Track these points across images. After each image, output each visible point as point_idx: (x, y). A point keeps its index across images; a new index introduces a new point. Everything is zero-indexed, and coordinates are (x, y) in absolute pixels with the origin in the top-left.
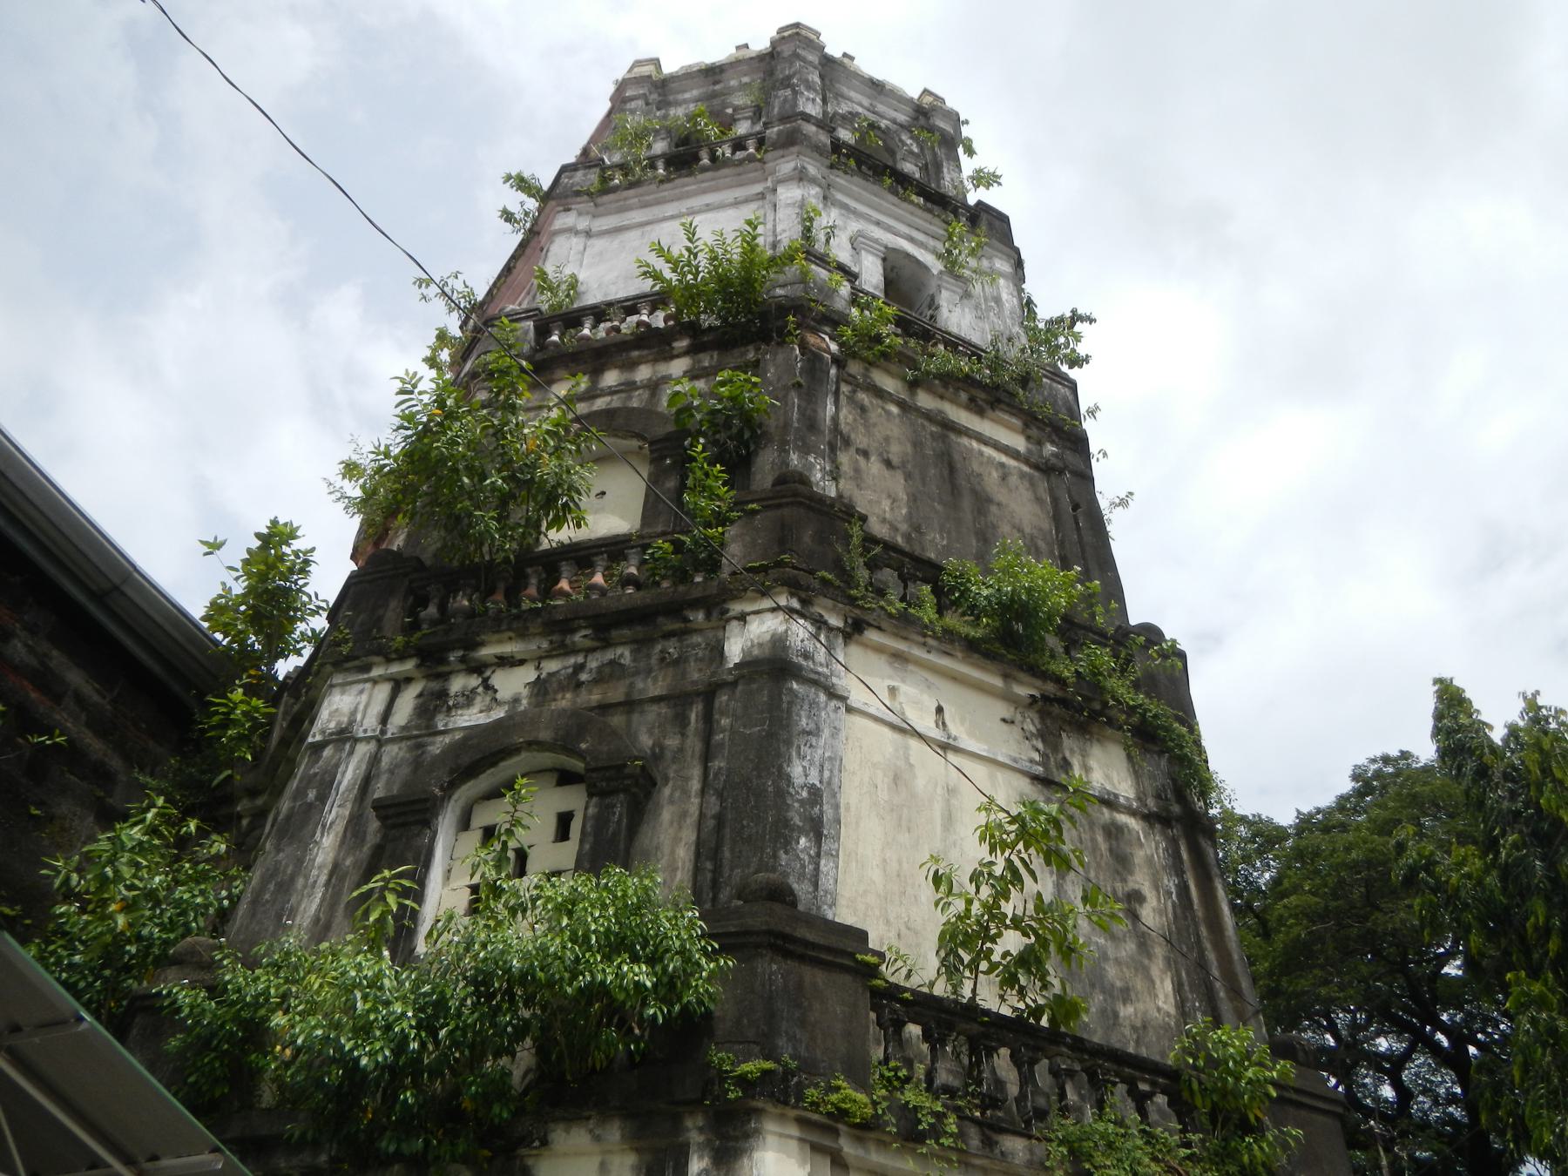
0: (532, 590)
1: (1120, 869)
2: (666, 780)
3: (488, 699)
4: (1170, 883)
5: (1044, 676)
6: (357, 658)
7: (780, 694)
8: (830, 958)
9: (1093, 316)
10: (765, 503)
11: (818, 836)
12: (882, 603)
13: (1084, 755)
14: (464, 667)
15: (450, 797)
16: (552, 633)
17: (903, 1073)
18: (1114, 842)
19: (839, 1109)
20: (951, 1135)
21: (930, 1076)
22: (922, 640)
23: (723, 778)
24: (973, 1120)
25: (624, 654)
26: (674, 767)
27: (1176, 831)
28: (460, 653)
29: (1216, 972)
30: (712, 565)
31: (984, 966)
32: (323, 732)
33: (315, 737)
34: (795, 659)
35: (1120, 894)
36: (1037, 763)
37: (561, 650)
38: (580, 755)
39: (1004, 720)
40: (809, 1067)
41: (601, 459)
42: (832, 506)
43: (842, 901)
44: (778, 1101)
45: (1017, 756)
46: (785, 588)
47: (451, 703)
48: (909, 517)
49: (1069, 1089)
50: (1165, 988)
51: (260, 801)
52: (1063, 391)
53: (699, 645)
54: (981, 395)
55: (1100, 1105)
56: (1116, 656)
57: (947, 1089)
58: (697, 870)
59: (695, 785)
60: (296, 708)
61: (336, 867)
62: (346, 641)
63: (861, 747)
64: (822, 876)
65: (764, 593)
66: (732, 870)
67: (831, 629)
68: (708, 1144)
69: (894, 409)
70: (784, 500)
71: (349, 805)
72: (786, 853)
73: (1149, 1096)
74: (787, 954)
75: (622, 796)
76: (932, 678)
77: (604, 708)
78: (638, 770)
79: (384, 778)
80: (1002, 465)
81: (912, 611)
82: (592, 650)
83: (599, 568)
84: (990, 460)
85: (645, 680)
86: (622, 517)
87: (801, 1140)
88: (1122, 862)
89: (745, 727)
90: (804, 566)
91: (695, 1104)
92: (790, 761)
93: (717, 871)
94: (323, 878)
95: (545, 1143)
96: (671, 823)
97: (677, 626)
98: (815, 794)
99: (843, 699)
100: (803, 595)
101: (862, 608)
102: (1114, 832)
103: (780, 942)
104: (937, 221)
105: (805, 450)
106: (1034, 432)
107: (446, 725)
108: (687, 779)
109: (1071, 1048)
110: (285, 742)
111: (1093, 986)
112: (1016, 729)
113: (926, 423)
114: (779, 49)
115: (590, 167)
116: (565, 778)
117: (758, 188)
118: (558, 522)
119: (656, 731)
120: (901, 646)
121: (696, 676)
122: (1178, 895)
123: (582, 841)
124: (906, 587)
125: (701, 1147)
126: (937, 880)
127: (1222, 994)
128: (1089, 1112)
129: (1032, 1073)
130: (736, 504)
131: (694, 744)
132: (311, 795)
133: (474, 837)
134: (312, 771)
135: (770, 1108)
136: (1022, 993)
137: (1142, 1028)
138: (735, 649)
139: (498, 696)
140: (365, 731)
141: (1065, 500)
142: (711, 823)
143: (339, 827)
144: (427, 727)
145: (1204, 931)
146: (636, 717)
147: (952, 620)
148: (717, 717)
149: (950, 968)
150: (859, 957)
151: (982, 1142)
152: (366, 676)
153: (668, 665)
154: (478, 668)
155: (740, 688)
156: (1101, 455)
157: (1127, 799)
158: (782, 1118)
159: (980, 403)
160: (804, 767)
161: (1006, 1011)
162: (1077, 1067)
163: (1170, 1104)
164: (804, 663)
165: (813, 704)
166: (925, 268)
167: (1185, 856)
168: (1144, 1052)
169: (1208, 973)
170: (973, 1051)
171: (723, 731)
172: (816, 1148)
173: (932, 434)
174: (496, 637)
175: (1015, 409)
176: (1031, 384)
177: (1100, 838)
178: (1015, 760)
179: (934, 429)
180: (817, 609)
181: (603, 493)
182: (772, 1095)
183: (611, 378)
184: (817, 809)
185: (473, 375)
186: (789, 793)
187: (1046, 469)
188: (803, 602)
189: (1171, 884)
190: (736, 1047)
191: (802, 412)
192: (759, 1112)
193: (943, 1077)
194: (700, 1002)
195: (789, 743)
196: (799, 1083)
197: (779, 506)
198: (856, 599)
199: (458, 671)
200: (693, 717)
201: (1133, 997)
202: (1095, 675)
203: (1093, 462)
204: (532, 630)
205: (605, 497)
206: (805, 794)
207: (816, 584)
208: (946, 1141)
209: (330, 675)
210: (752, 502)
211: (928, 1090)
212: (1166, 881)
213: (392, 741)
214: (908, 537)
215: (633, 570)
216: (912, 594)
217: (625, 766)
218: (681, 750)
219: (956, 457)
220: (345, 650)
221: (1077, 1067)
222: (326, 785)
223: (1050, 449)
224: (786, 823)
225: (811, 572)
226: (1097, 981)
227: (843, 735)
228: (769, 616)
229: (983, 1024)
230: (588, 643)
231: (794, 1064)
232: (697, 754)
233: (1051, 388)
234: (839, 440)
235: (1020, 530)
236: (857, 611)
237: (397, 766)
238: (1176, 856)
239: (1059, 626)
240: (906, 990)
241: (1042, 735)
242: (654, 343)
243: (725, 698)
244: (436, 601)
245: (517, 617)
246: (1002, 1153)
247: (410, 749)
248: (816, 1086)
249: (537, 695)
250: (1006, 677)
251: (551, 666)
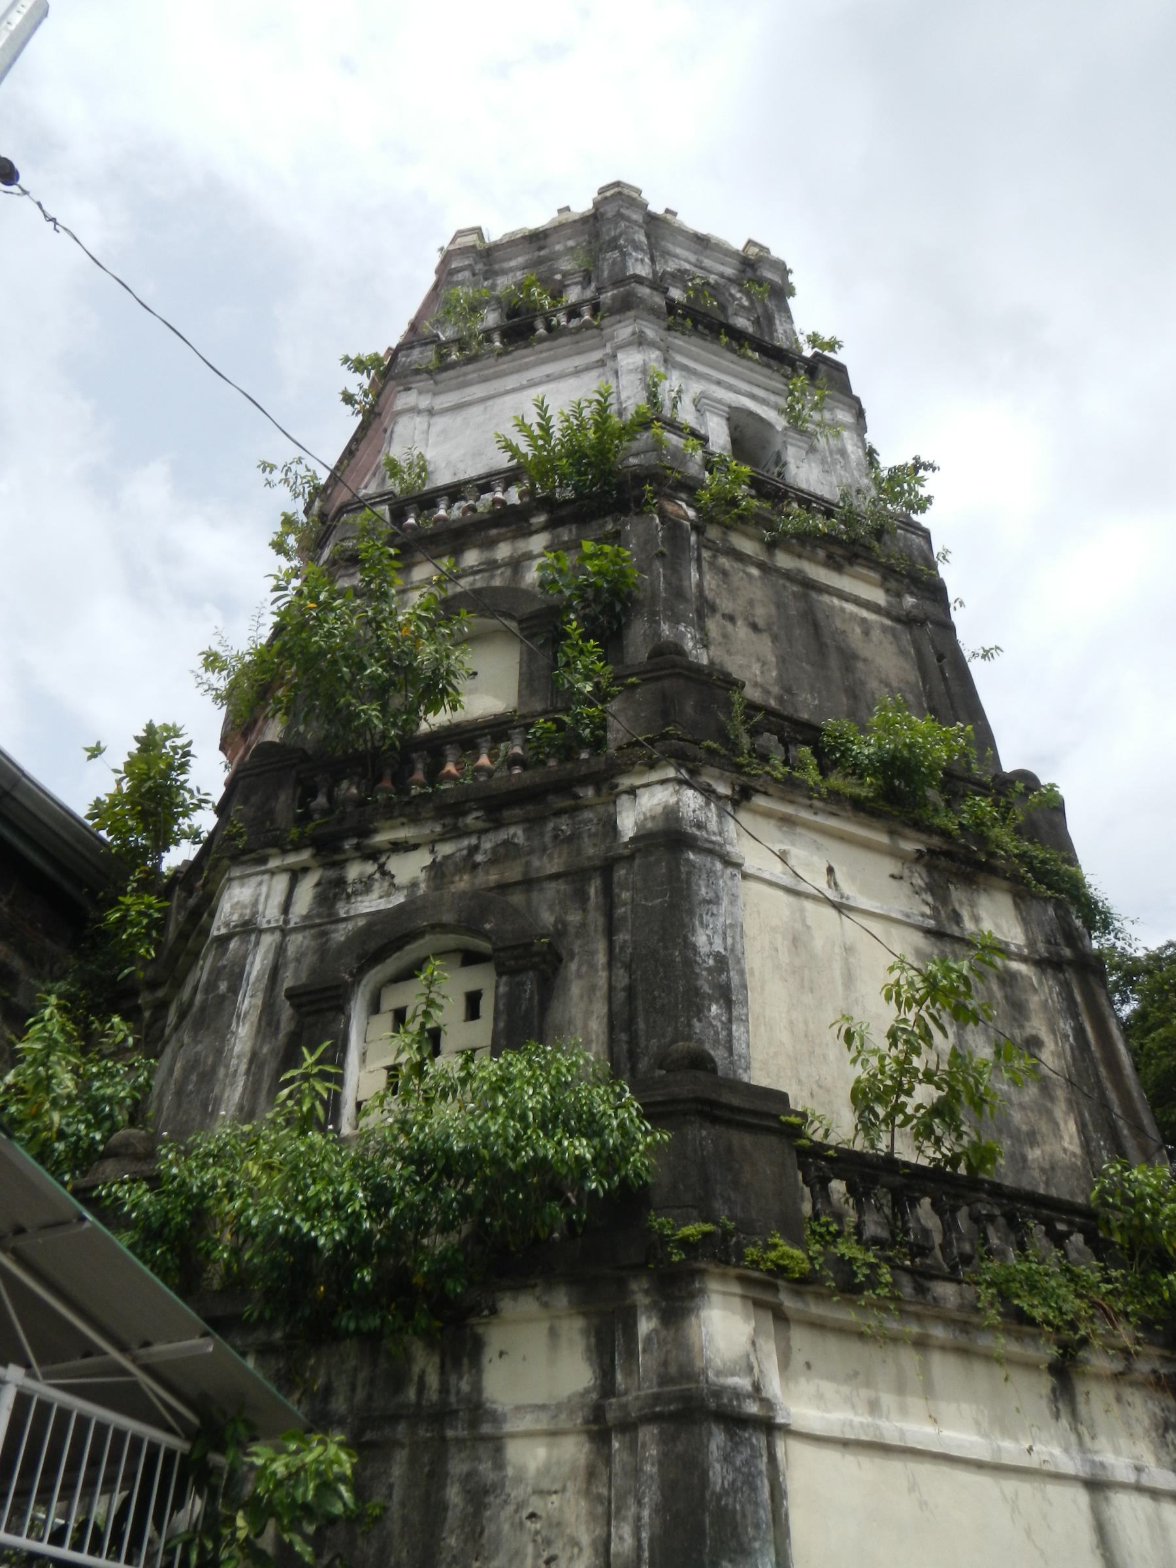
0: (419, 775)
1: (1017, 1016)
2: (572, 956)
3: (386, 884)
4: (1066, 1026)
5: (930, 830)
6: (252, 851)
7: (678, 865)
8: (755, 1121)
9: (936, 465)
10: (645, 676)
11: (728, 1004)
12: (768, 769)
13: (973, 905)
14: (358, 854)
15: (359, 982)
16: (443, 817)
17: (834, 1228)
18: (1009, 990)
19: (778, 1266)
20: (886, 1285)
21: (859, 1229)
22: (808, 802)
23: (629, 951)
24: (905, 1269)
25: (517, 833)
26: (579, 942)
27: (1070, 975)
28: (355, 841)
29: (1117, 1110)
30: (598, 744)
31: (899, 1119)
32: (227, 925)
33: (218, 929)
34: (689, 830)
35: (1019, 1040)
36: (929, 917)
38: (485, 935)
39: (893, 876)
40: (746, 1227)
41: (472, 639)
42: (710, 675)
43: (755, 1065)
44: (721, 1261)
45: (909, 911)
46: (672, 760)
47: (350, 890)
48: (780, 680)
49: (991, 1231)
50: (1070, 1127)
51: (160, 993)
52: (917, 541)
53: (591, 820)
54: (839, 551)
55: (1021, 1246)
56: (996, 804)
57: (876, 1241)
58: (612, 1043)
59: (601, 959)
60: (192, 902)
61: (254, 1056)
62: (241, 835)
63: (759, 913)
64: (735, 1041)
65: (652, 766)
66: (648, 1041)
67: (720, 797)
68: (654, 1305)
69: (755, 572)
70: (662, 673)
71: (260, 995)
72: (700, 1020)
73: (1067, 1235)
74: (715, 1120)
75: (531, 974)
76: (820, 839)
77: (503, 887)
78: (545, 948)
79: (292, 966)
80: (864, 621)
81: (796, 774)
82: (485, 831)
83: (484, 750)
84: (853, 617)
85: (541, 858)
86: (496, 697)
87: (743, 1297)
88: (1018, 1009)
89: (646, 900)
90: (689, 737)
91: (638, 1269)
92: (694, 930)
93: (633, 1041)
94: (243, 1067)
95: (494, 1311)
96: (582, 997)
97: (568, 803)
98: (721, 962)
99: (738, 866)
100: (691, 766)
101: (749, 775)
102: (1008, 979)
103: (707, 1109)
104: (776, 375)
105: (675, 620)
106: (893, 584)
107: (347, 912)
108: (592, 953)
109: (990, 1194)
110: (183, 936)
111: (1000, 1131)
112: (905, 885)
113: (788, 584)
114: (602, 210)
115: (426, 344)
116: (470, 958)
117: (597, 355)
118: (434, 707)
119: (557, 908)
120: (789, 810)
121: (591, 851)
122: (1075, 1039)
123: (496, 1020)
124: (787, 751)
125: (649, 1309)
126: (849, 1037)
127: (1125, 1132)
128: (1012, 1253)
129: (955, 1220)
130: (615, 678)
131: (596, 919)
132: (223, 987)
133: (385, 1020)
134: (220, 964)
135: (712, 1268)
136: (938, 1142)
137: (1050, 1170)
138: (628, 823)
139: (396, 881)
140: (269, 922)
141: (929, 651)
142: (621, 996)
143: (254, 1017)
144: (330, 915)
145: (1103, 1071)
146: (535, 895)
147: (836, 780)
148: (617, 891)
149: (866, 1125)
150: (783, 1118)
151: (915, 1289)
152: (263, 868)
153: (562, 841)
154: (373, 855)
155: (637, 862)
156: (957, 604)
157: (1018, 946)
158: (724, 1277)
159: (838, 559)
160: (708, 936)
161: (924, 1162)
162: (997, 1212)
163: (1086, 1242)
164: (698, 833)
165: (711, 873)
166: (768, 425)
167: (1079, 998)
168: (1054, 1193)
169: (1111, 1110)
170: (897, 1203)
171: (625, 904)
172: (758, 1304)
173: (794, 593)
174: (389, 823)
175: (874, 564)
176: (886, 537)
177: (995, 987)
178: (908, 916)
179: (795, 589)
180: (705, 779)
181: (475, 674)
182: (714, 1256)
183: (471, 558)
184: (724, 976)
185: (332, 562)
186: (696, 962)
187: (908, 621)
188: (693, 772)
189: (1068, 1027)
190: (676, 1212)
191: (668, 583)
192: (702, 1273)
193: (872, 1228)
194: (638, 1175)
195: (691, 913)
196: (738, 1243)
197: (659, 678)
198: (742, 766)
199: (353, 859)
200: (592, 891)
201: (1039, 1138)
202: (978, 825)
203: (952, 609)
204: (424, 815)
205: (477, 677)
206: (711, 962)
207: (702, 754)
208: (883, 1292)
209: (228, 869)
210: (631, 675)
211: (858, 1242)
212: (1062, 1024)
213: (296, 930)
214: (780, 699)
215: (518, 750)
216: (795, 758)
217: (532, 944)
218: (583, 925)
219: (820, 616)
220: (240, 843)
221: (997, 1212)
222: (236, 976)
223: (909, 601)
224: (697, 991)
225: (696, 743)
226: (1005, 1127)
227: (740, 902)
228: (659, 788)
229: (904, 1175)
230: (481, 825)
231: (731, 1225)
232: (600, 928)
233: (906, 539)
234: (705, 608)
235: (888, 685)
236: (744, 779)
237: (303, 954)
238: (1070, 1000)
239: (942, 781)
240: (830, 1147)
241: (930, 888)
243: (623, 872)
244: (324, 790)
245: (409, 803)
246: (934, 1299)
247: (315, 937)
248: (755, 1245)
249: (435, 877)
250: (892, 833)
251: (446, 849)
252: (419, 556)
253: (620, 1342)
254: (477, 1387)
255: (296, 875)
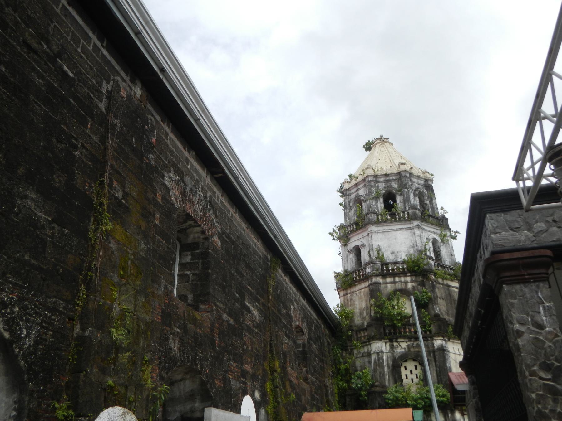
37: (410, 341)
59: (434, 365)
65: (439, 336)
69: (441, 286)
94: (387, 374)
117: (408, 226)
188: (444, 338)
207: (445, 335)
242: (403, 273)
251: (409, 343)
252: (388, 276)
253: (447, 416)
254: (431, 419)
255: (386, 343)
